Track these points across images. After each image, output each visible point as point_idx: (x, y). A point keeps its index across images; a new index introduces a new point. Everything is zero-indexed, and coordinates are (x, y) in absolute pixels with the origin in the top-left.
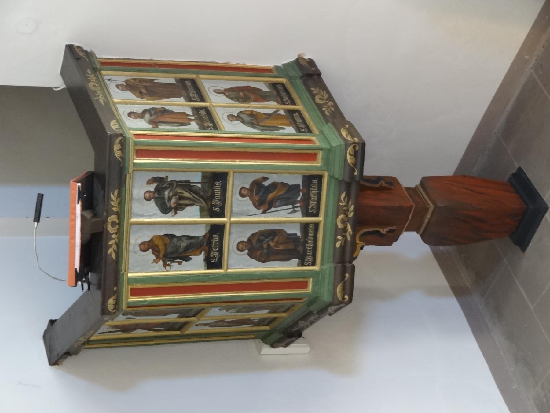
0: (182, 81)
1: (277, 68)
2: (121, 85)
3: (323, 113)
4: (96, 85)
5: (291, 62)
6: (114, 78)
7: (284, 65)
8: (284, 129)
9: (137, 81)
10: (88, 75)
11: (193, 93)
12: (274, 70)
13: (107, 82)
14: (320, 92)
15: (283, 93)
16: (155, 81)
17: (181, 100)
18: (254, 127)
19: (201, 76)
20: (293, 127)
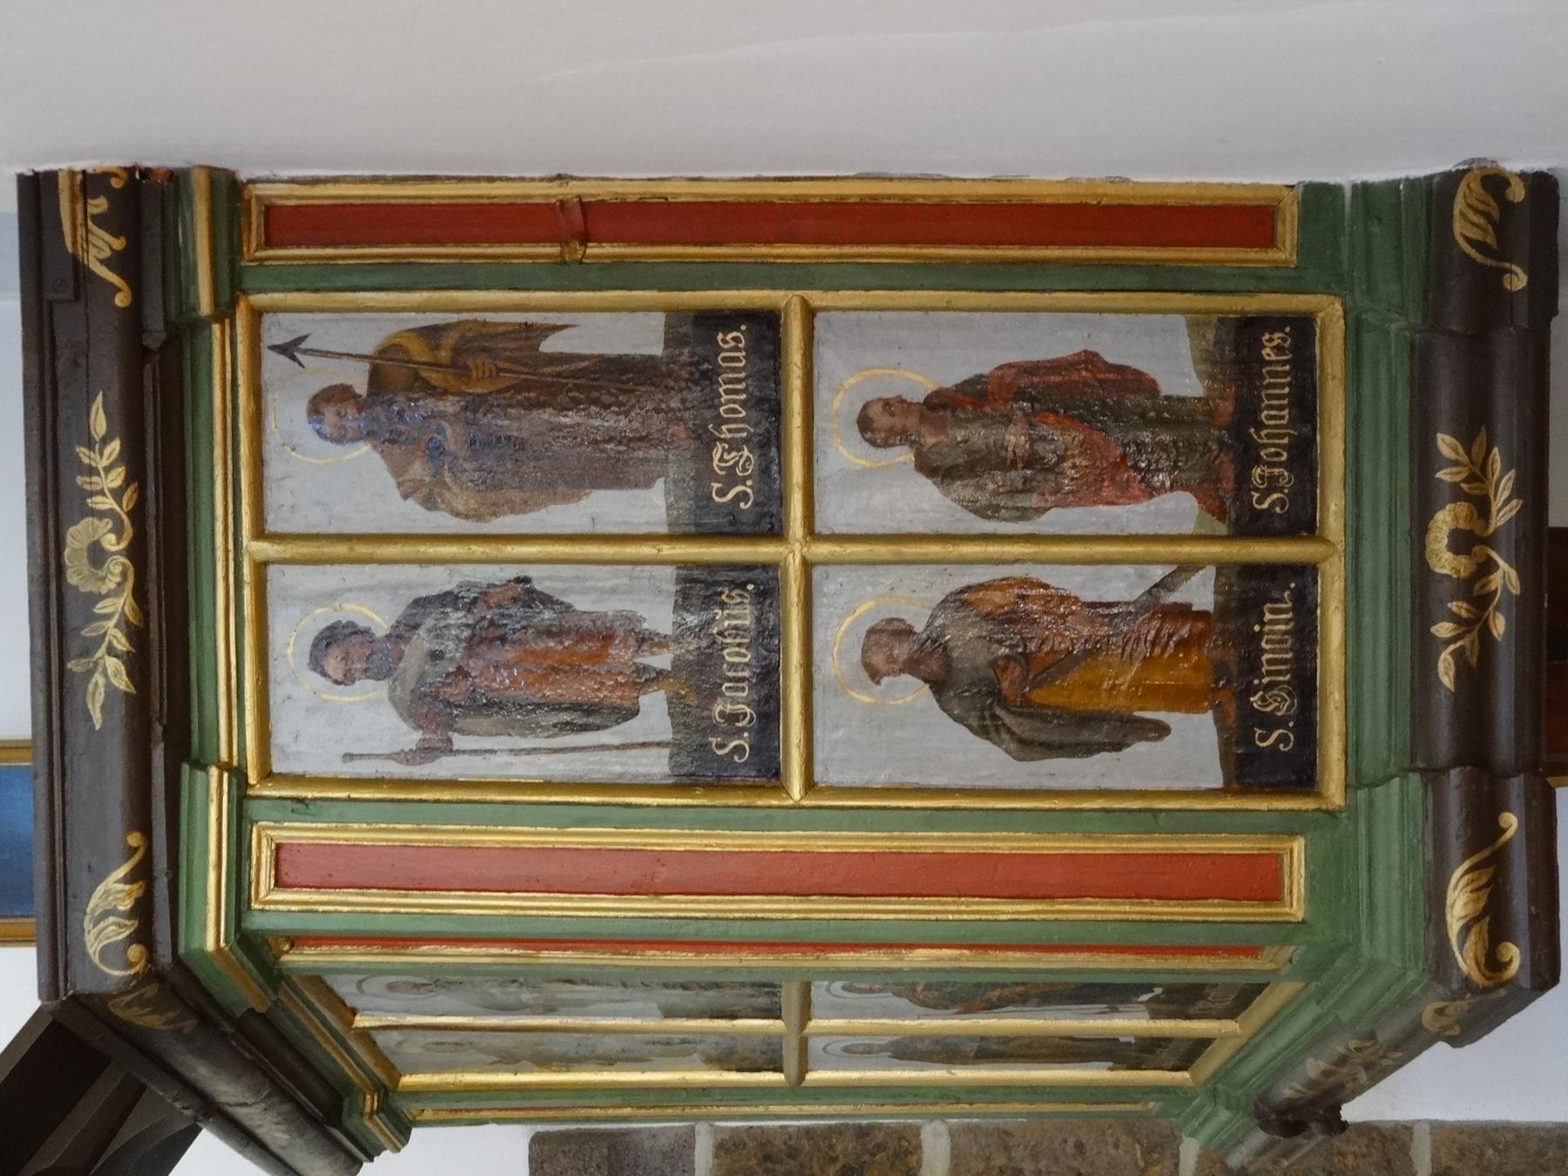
0: (714, 320)
1: (1318, 197)
2: (337, 395)
3: (1425, 649)
4: (110, 542)
5: (1412, 183)
6: (322, 331)
7: (1364, 192)
8: (1162, 730)
9: (444, 355)
10: (82, 451)
11: (734, 446)
12: (1288, 230)
13: (273, 363)
14: (1479, 474)
15: (1275, 416)
16: (550, 346)
17: (647, 506)
18: (987, 729)
19: (817, 298)
20: (1220, 722)
